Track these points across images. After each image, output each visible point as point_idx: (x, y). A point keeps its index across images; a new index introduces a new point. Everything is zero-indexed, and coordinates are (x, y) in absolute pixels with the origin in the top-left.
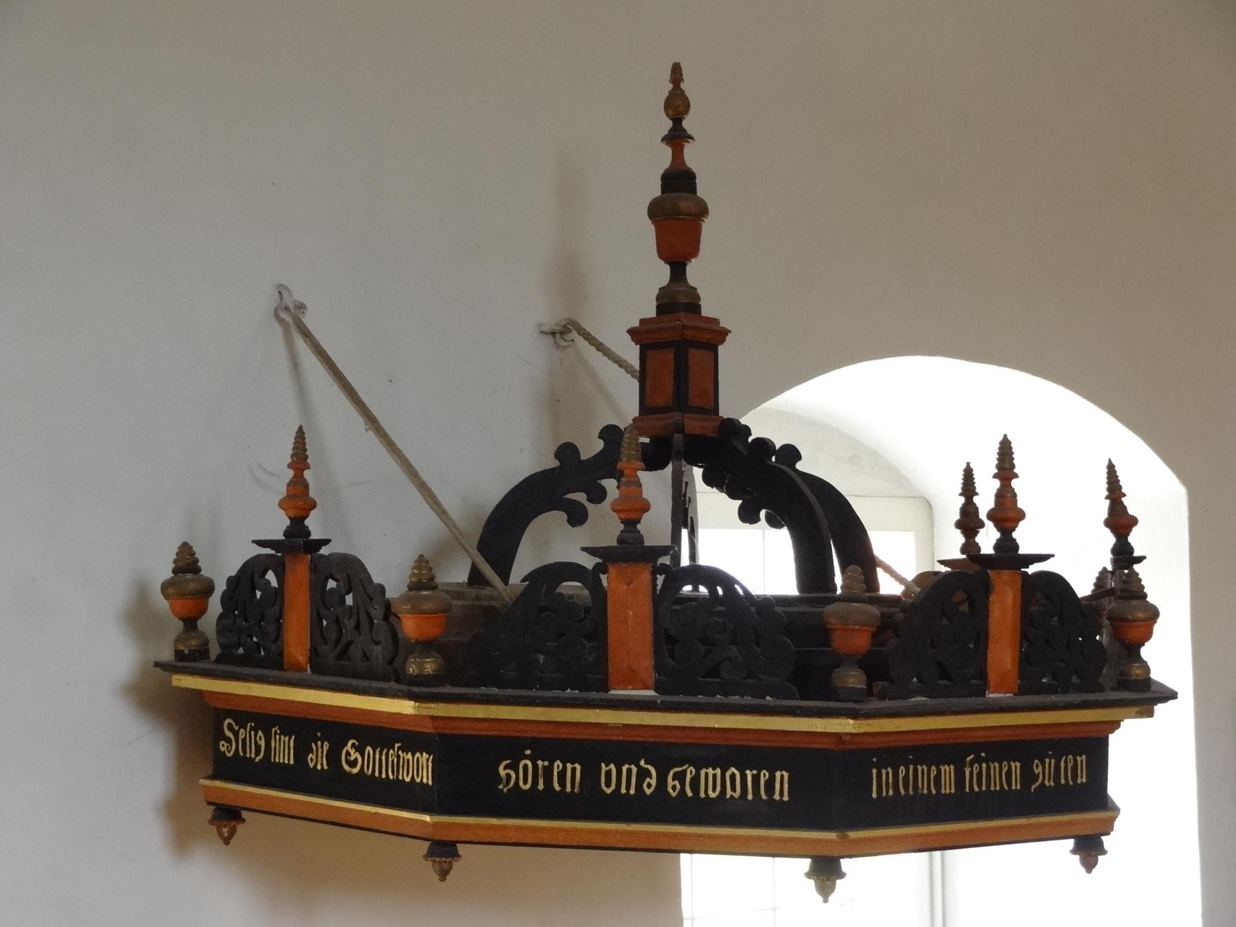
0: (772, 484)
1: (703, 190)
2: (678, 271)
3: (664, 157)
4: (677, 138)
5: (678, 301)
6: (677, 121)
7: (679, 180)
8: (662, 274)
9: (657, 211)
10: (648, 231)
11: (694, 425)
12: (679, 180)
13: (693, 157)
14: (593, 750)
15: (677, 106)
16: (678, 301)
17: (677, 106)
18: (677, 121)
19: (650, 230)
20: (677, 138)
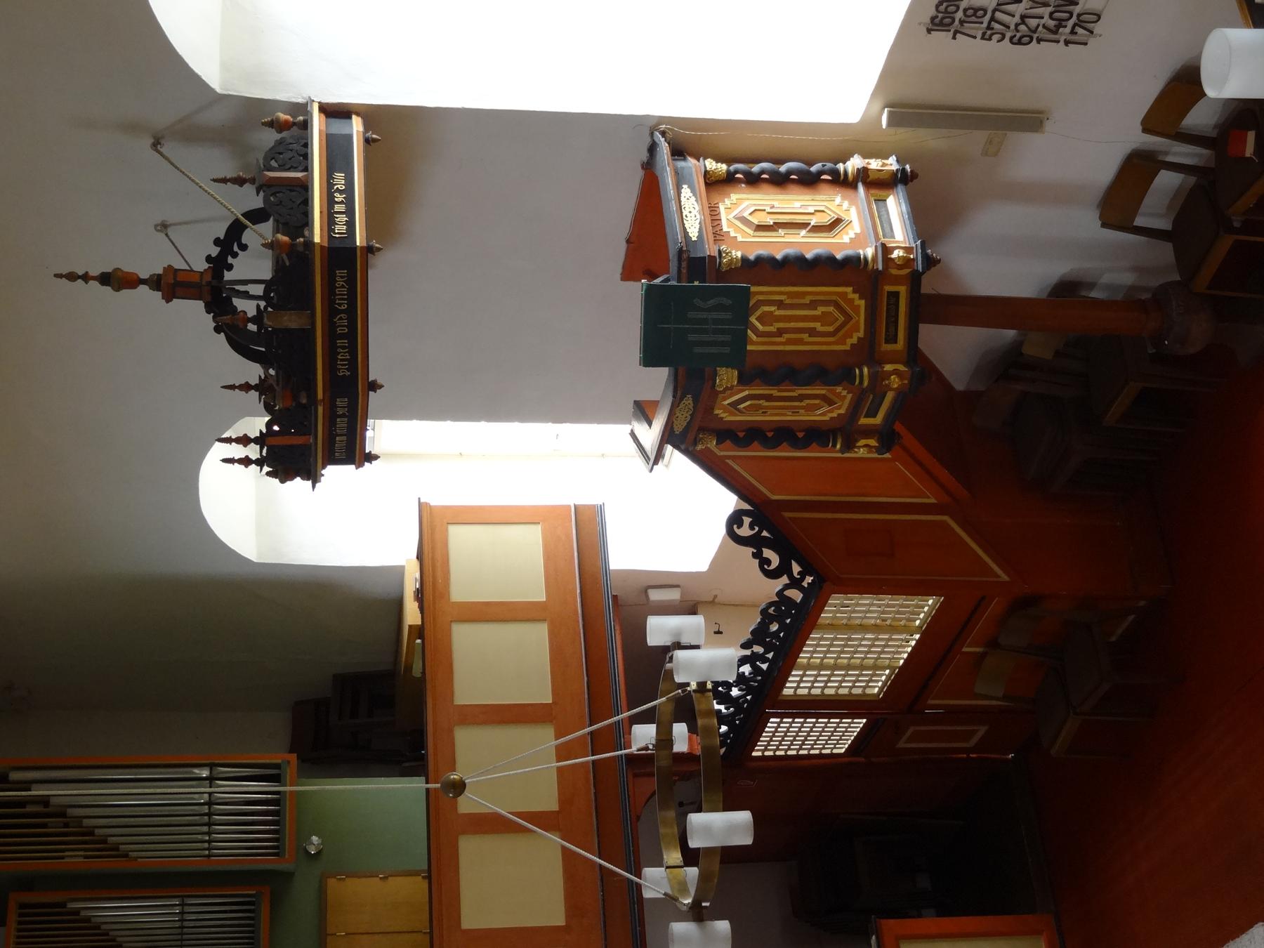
0: (231, 241)
1: (108, 269)
2: (143, 282)
3: (94, 284)
4: (86, 278)
5: (155, 282)
6: (79, 277)
7: (105, 279)
8: (143, 289)
9: (118, 290)
10: (125, 292)
11: (208, 278)
12: (105, 279)
13: (94, 272)
14: (331, 336)
15: (72, 277)
16: (155, 282)
17: (72, 277)
18: (79, 277)
19: (124, 291)
20: (86, 278)
